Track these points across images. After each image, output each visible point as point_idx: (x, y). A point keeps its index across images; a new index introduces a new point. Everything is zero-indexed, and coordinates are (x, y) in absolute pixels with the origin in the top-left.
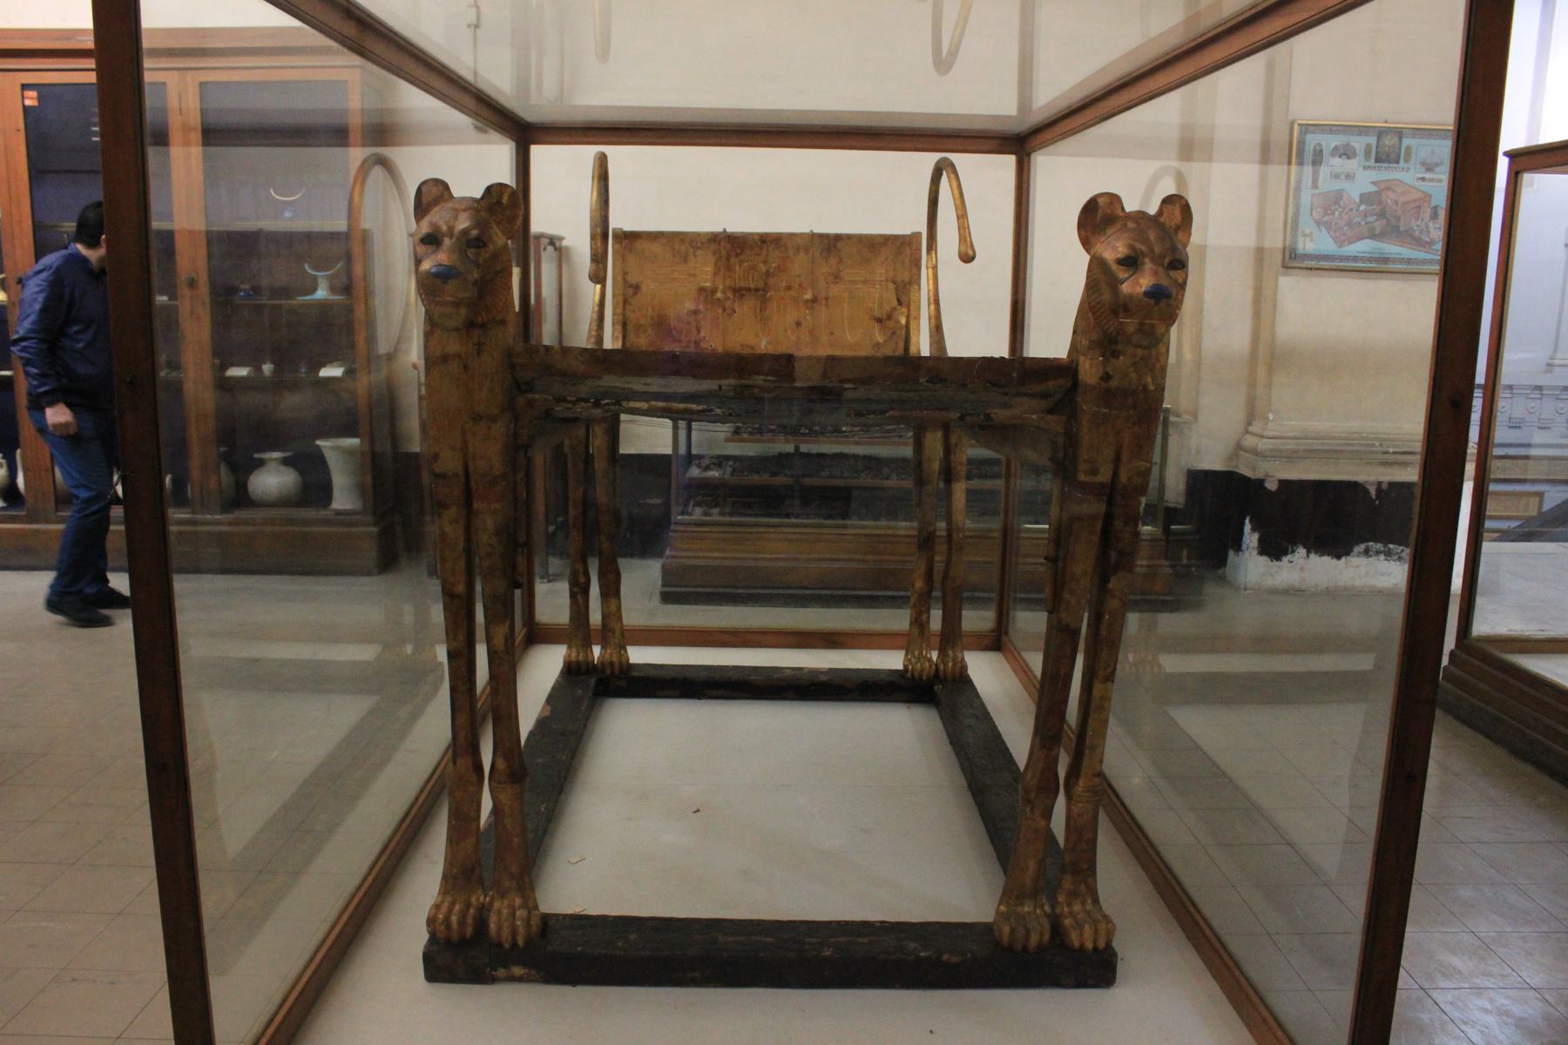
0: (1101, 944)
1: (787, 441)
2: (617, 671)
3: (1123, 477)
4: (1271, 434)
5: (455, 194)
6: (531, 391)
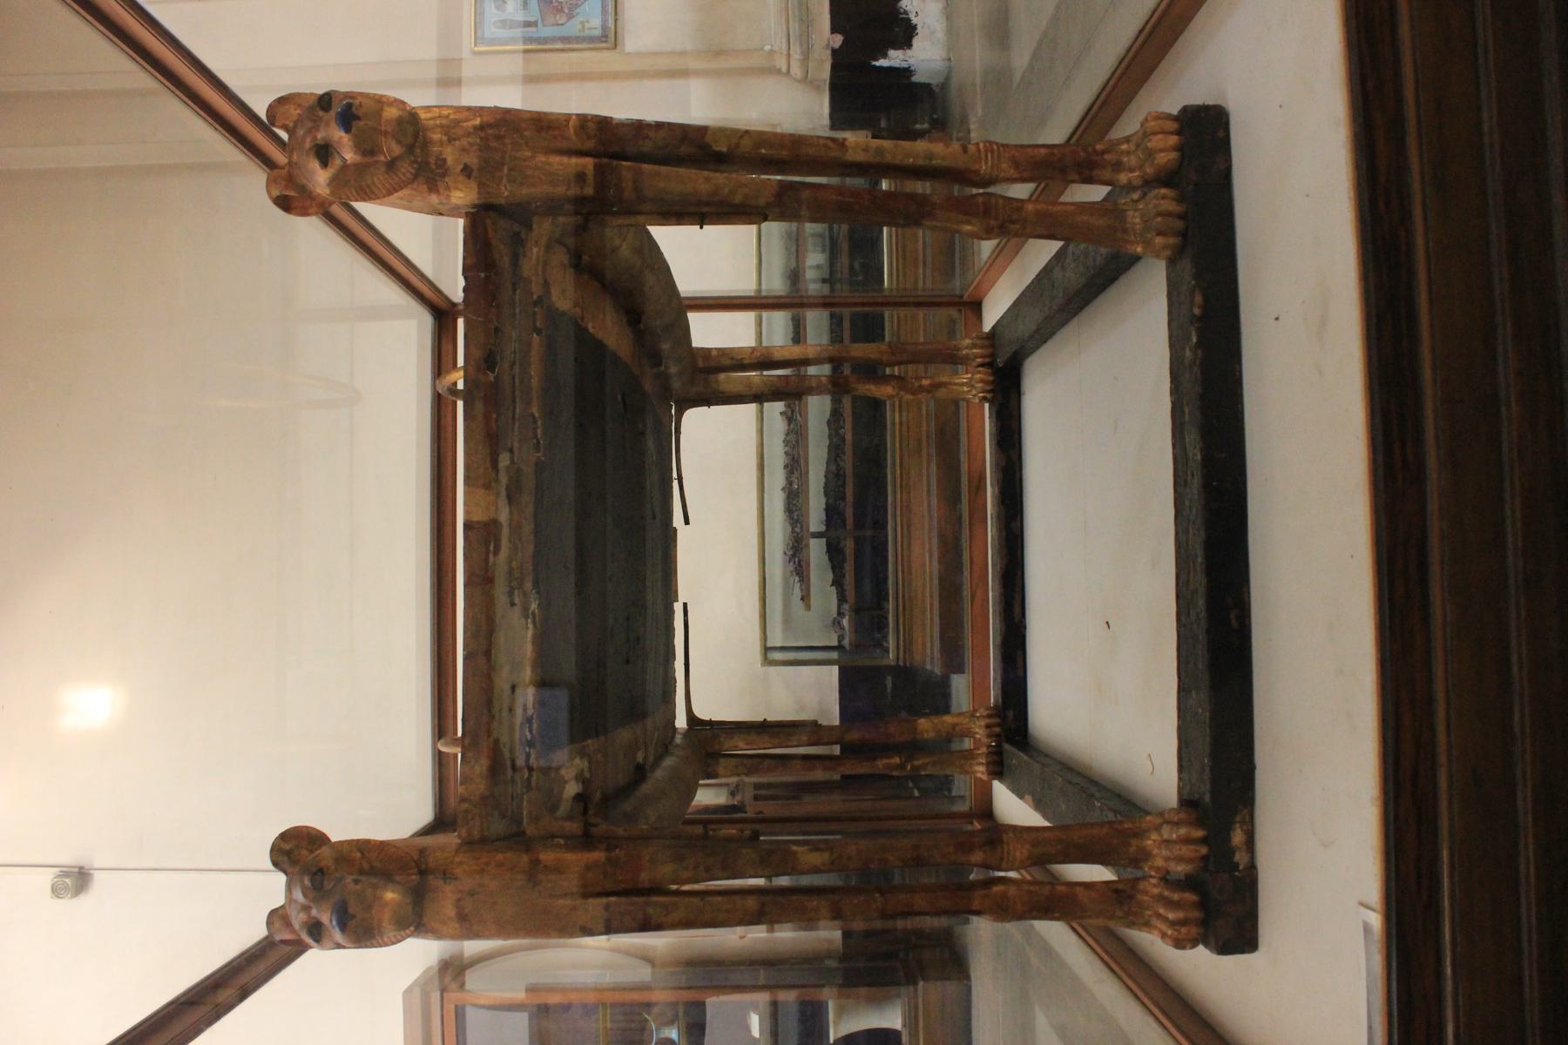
0: (1174, 126)
1: (807, 546)
2: (997, 720)
3: (590, 145)
4: (784, 46)
5: (279, 900)
6: (520, 822)
